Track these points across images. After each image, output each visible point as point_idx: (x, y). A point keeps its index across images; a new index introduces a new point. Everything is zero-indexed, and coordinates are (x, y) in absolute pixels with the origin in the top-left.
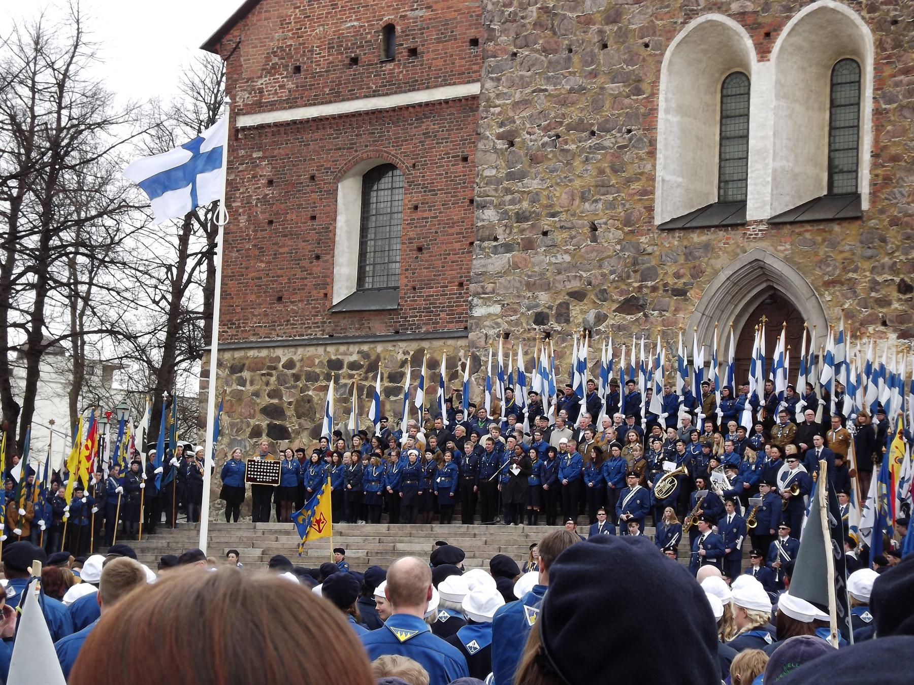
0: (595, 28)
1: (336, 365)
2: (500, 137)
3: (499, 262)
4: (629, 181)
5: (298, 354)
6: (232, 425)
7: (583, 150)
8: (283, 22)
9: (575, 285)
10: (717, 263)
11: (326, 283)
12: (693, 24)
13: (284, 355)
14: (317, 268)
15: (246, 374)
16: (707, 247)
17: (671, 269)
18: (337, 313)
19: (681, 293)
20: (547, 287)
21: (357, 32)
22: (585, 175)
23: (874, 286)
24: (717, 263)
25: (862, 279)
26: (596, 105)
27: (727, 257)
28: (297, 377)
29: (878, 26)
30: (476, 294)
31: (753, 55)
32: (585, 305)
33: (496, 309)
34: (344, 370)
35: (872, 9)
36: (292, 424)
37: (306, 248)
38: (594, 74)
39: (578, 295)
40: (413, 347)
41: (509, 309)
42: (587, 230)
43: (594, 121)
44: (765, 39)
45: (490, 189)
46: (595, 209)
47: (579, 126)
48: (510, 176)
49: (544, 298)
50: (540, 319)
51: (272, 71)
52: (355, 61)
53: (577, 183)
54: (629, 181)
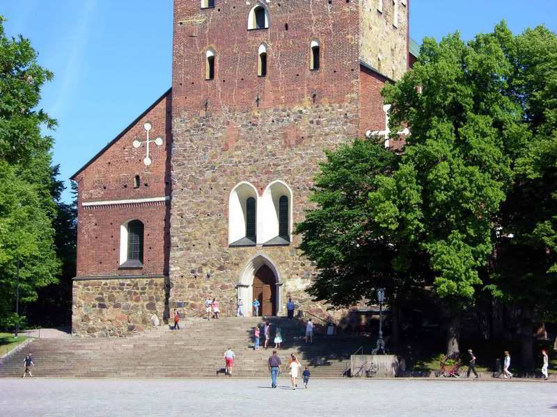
0: (208, 183)
1: (123, 284)
2: (178, 215)
3: (178, 254)
4: (220, 230)
5: (108, 281)
6: (85, 304)
7: (204, 220)
8: (99, 172)
9: (204, 262)
10: (248, 256)
11: (117, 257)
12: (239, 184)
13: (104, 282)
14: (114, 253)
15: (89, 287)
16: (245, 251)
17: (234, 258)
18: (120, 269)
19: (237, 264)
20: (195, 262)
21: (126, 177)
22: (206, 228)
23: (294, 264)
24: (248, 256)
25: (290, 262)
26: (209, 208)
27: (251, 254)
28: (108, 288)
29: (294, 189)
30: (172, 264)
31: (258, 195)
32: (207, 268)
33: (178, 268)
34: (125, 286)
35: (292, 184)
36: (107, 303)
37: (110, 246)
38: (208, 197)
39: (205, 265)
40: (149, 280)
41: (182, 269)
42: (208, 245)
43: (209, 211)
44: (262, 189)
45: (175, 231)
46: (210, 238)
47: (204, 213)
48: (181, 227)
49: (194, 265)
50: (193, 272)
51: (95, 188)
52: (126, 186)
53: (204, 230)
54: (220, 230)
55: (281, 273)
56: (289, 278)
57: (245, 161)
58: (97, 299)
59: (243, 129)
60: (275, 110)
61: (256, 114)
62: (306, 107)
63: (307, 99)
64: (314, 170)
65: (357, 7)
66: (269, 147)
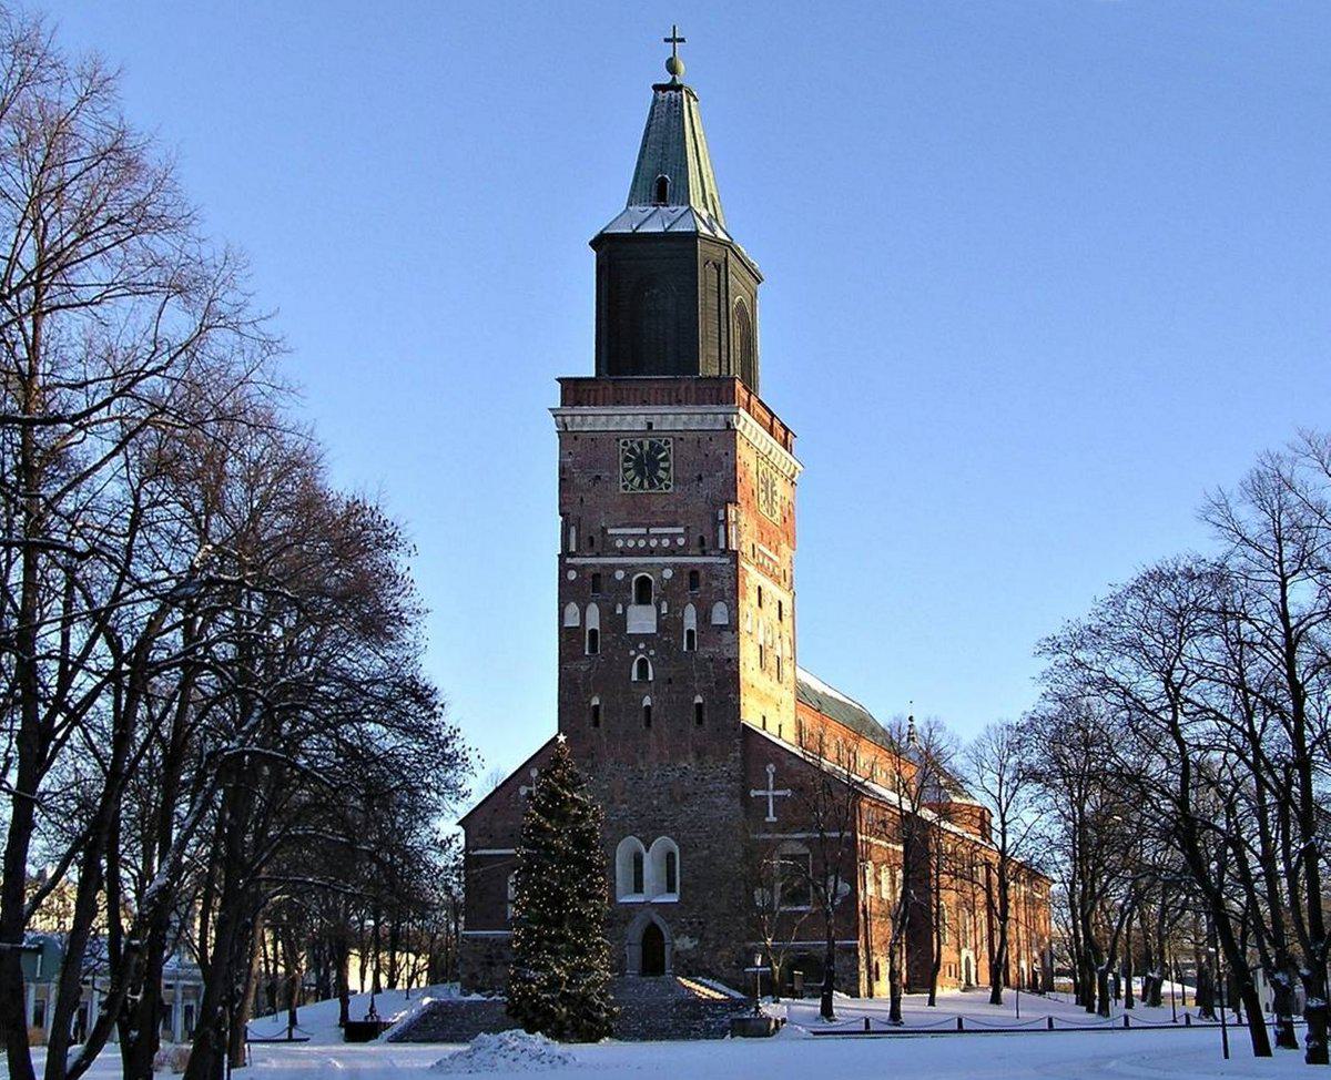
55: (666, 931)
56: (677, 937)
57: (631, 815)
58: (486, 956)
59: (630, 783)
60: (661, 764)
61: (642, 768)
62: (689, 763)
63: (691, 757)
64: (700, 827)
65: (738, 667)
66: (655, 802)
